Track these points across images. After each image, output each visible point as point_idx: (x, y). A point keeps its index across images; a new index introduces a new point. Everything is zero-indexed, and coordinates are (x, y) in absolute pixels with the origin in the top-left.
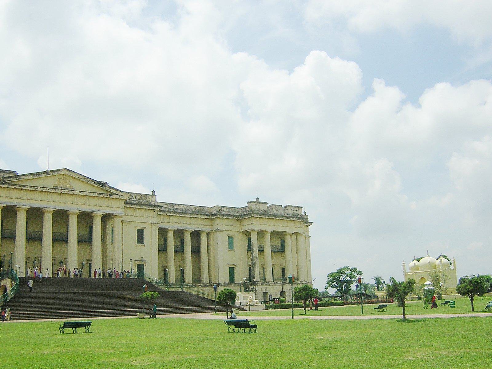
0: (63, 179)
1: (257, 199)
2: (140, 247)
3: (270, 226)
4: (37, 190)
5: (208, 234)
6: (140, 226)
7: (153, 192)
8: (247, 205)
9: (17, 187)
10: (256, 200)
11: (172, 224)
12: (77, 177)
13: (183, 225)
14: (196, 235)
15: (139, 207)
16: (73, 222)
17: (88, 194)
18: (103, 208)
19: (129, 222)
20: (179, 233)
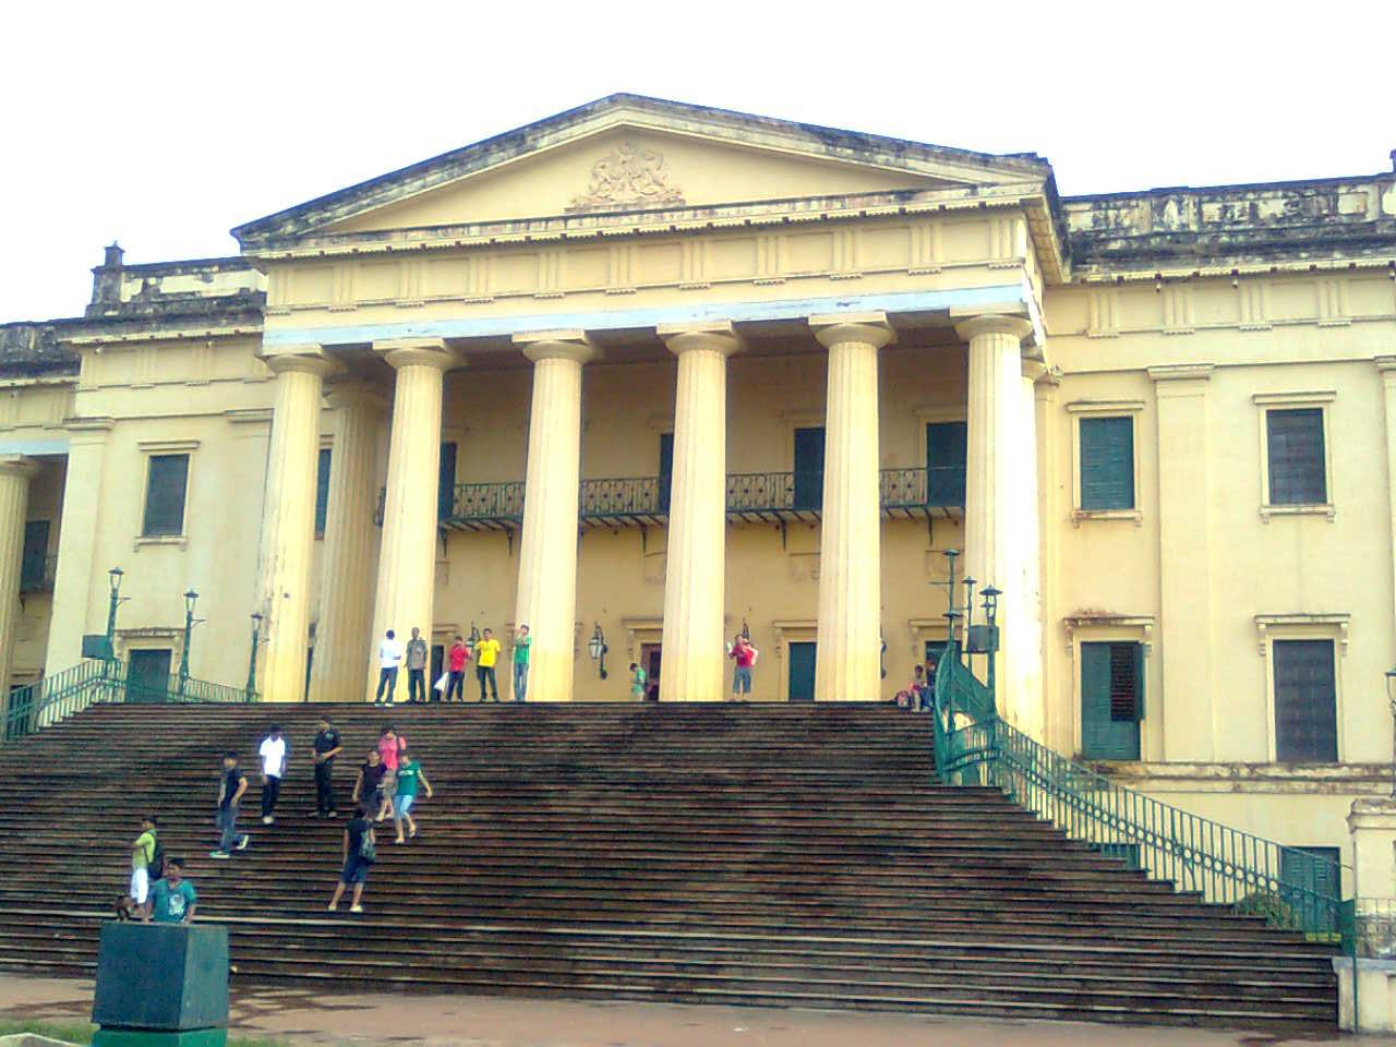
0: (623, 158)
2: (1297, 530)
4: (465, 241)
6: (1293, 387)
9: (365, 247)
12: (691, 128)
15: (1267, 267)
16: (702, 400)
17: (758, 215)
19: (1198, 376)
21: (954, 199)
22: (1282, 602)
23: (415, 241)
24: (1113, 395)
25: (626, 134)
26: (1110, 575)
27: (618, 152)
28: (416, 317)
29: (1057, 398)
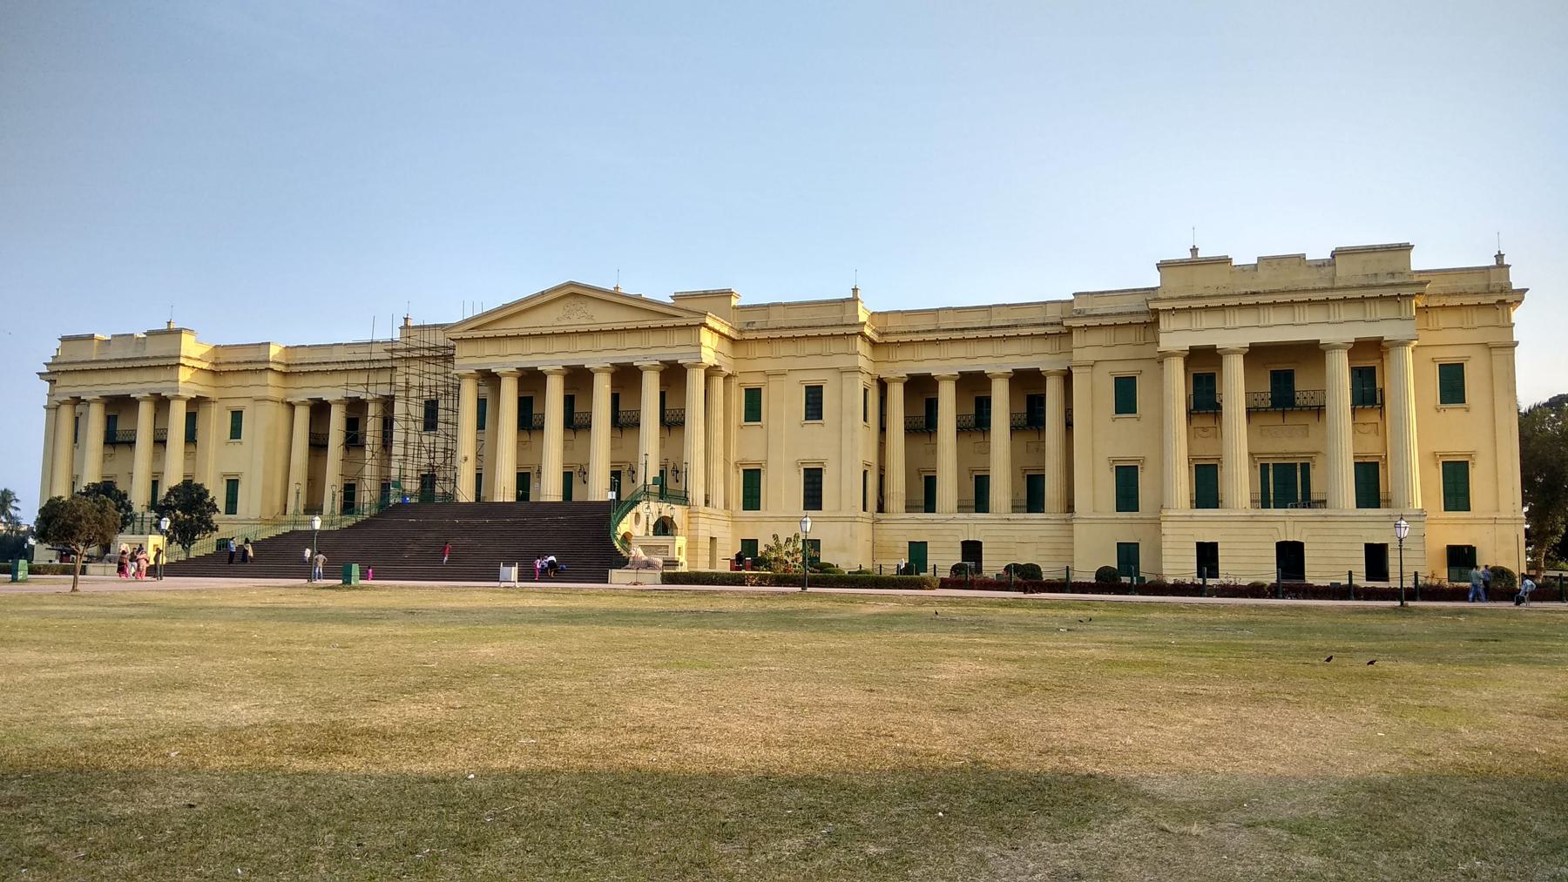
1: (1194, 250)
2: (814, 426)
3: (1233, 335)
5: (1067, 378)
6: (813, 379)
7: (855, 290)
8: (1153, 280)
10: (1188, 256)
11: (944, 364)
13: (978, 361)
14: (1028, 385)
18: (653, 352)
20: (974, 386)
22: (807, 456)
23: (503, 333)
24: (753, 382)
26: (750, 445)
27: (571, 300)
28: (507, 360)
29: (734, 382)
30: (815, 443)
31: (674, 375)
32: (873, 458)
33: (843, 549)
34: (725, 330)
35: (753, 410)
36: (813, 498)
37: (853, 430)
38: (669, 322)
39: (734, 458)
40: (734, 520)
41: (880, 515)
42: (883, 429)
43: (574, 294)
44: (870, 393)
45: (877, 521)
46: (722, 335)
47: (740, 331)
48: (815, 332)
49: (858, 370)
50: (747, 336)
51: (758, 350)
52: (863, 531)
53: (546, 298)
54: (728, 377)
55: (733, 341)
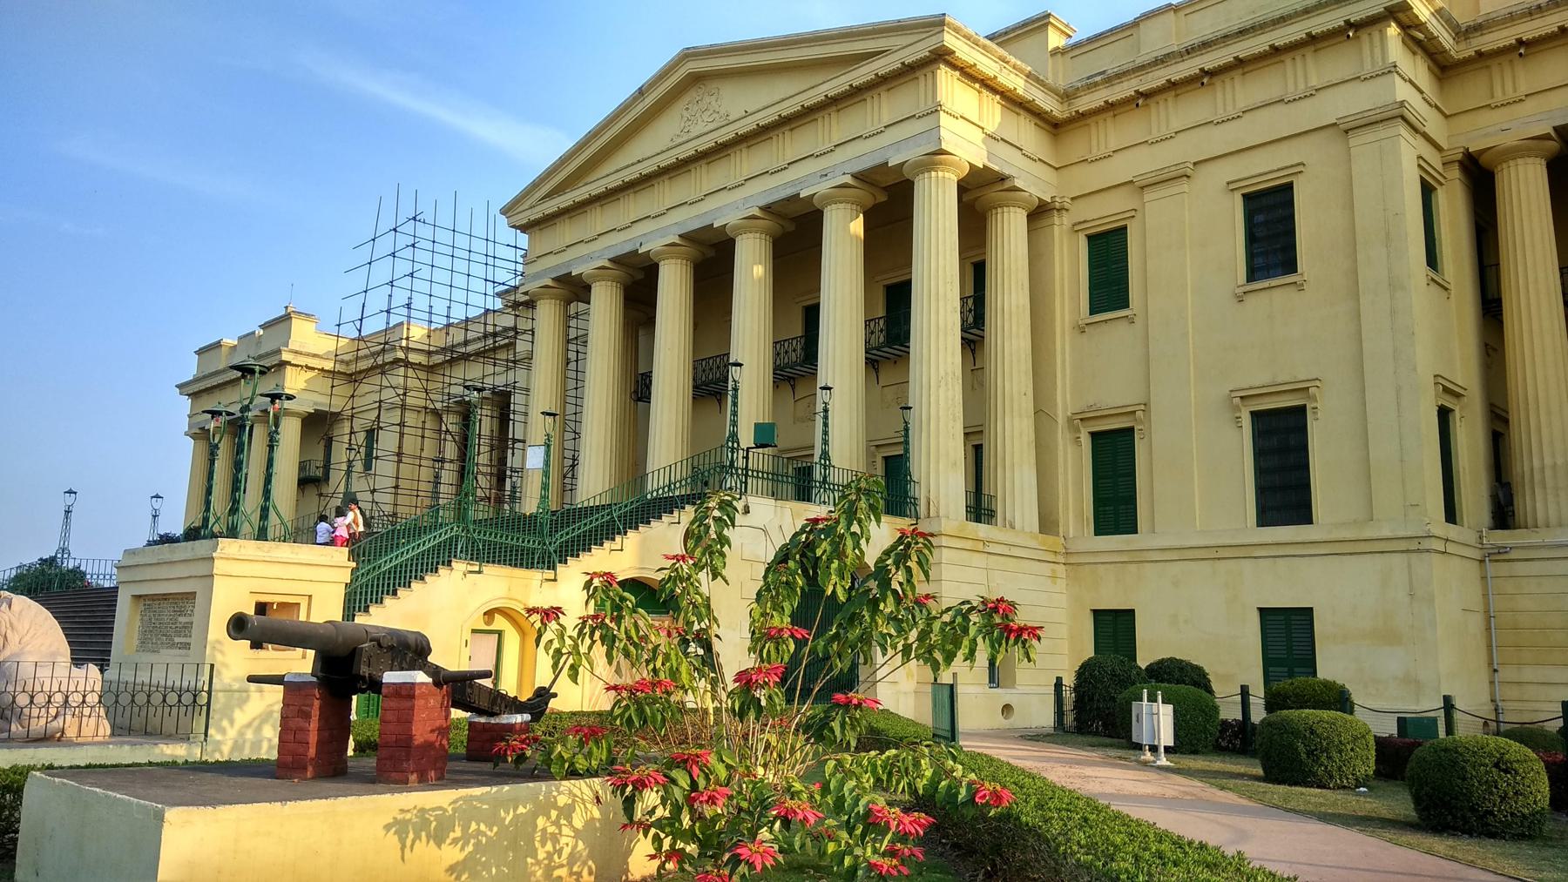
6: (1262, 169)
21: (882, 66)
22: (1256, 376)
25: (696, 79)
27: (693, 95)
30: (1280, 341)
31: (889, 204)
32: (1466, 372)
33: (1388, 636)
34: (1016, 83)
35: (1109, 282)
36: (1283, 488)
37: (1395, 285)
38: (862, 74)
39: (1065, 403)
40: (1071, 561)
41: (1502, 537)
42: (1491, 308)
43: (693, 76)
44: (1441, 198)
45: (1497, 554)
46: (1012, 102)
47: (1067, 96)
48: (1259, 44)
49: (1399, 115)
50: (1086, 103)
51: (1111, 134)
52: (1451, 585)
53: (650, 100)
54: (1039, 213)
55: (1054, 127)
